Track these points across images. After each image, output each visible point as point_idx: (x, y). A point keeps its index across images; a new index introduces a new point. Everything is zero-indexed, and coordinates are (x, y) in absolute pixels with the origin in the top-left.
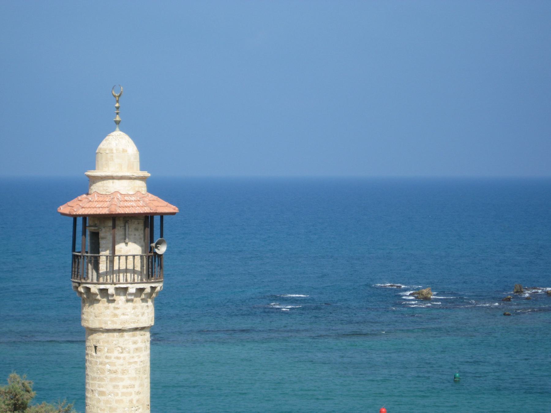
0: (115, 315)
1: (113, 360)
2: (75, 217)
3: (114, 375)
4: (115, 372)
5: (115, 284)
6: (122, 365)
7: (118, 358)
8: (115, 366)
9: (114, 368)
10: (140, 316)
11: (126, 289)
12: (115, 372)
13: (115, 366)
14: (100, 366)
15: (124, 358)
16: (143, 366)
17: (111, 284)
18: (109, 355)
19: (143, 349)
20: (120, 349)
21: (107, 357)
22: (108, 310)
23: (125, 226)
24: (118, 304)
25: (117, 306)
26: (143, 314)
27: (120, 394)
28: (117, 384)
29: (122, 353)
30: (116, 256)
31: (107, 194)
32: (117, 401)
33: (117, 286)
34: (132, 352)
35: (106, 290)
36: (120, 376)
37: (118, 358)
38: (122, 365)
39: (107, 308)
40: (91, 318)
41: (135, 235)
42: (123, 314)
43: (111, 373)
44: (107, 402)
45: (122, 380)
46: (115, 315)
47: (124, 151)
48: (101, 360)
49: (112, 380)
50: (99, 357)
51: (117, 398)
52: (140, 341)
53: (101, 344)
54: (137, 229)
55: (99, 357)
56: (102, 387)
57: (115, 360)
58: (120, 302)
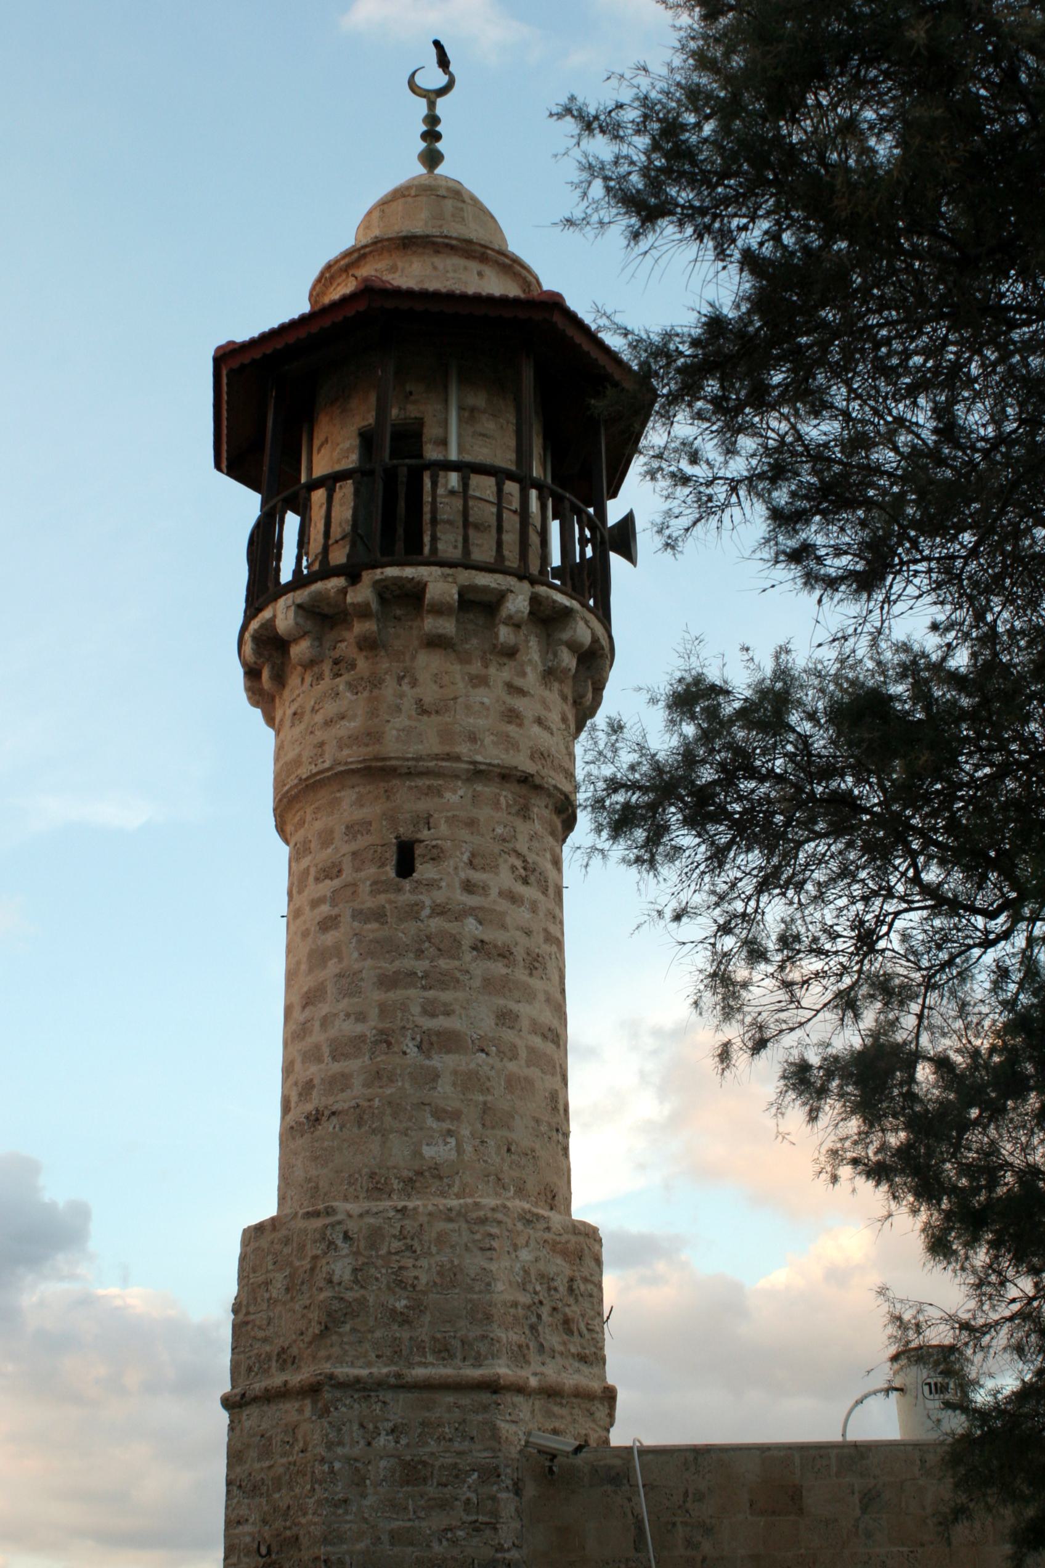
1: (492, 900)
3: (498, 968)
7: (513, 898)
8: (504, 927)
13: (504, 927)
18: (477, 876)
21: (469, 887)
22: (481, 691)
24: (524, 674)
25: (518, 682)
32: (512, 1083)
35: (501, 596)
36: (520, 974)
39: (480, 681)
40: (401, 721)
43: (489, 956)
44: (470, 1081)
46: (513, 716)
48: (439, 896)
49: (491, 985)
50: (431, 885)
51: (512, 1067)
53: (443, 828)
55: (431, 885)
56: (447, 1014)
57: (504, 905)
58: (528, 669)
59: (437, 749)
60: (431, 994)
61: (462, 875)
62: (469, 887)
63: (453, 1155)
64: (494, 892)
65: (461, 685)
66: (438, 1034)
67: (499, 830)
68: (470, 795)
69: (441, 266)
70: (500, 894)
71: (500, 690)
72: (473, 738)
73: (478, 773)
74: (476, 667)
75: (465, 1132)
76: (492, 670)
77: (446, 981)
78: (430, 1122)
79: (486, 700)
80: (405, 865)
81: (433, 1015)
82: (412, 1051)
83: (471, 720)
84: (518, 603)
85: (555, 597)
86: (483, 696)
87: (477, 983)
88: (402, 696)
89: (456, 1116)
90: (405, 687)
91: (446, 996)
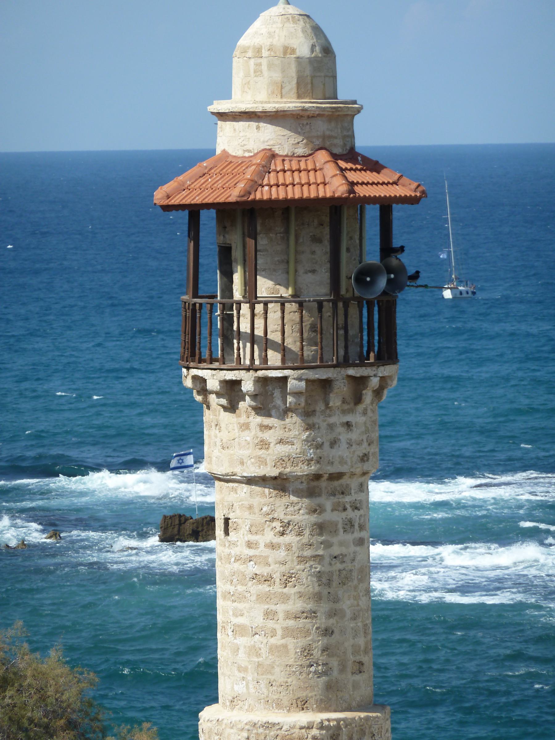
0: (264, 445)
1: (262, 550)
2: (194, 212)
3: (265, 588)
4: (268, 579)
5: (256, 370)
6: (284, 563)
7: (273, 546)
9: (264, 571)
10: (327, 445)
11: (285, 379)
12: (268, 579)
14: (237, 566)
15: (289, 548)
16: (339, 566)
17: (248, 370)
19: (340, 526)
20: (277, 524)
21: (249, 545)
22: (247, 432)
23: (287, 232)
26: (333, 443)
27: (279, 632)
28: (273, 607)
29: (282, 534)
30: (259, 303)
31: (247, 155)
33: (261, 373)
34: (307, 532)
35: (238, 383)
37: (273, 546)
38: (284, 563)
39: (245, 427)
41: (313, 253)
42: (281, 441)
43: (259, 582)
45: (285, 598)
46: (264, 445)
47: (287, 50)
50: (235, 544)
52: (328, 505)
53: (238, 511)
54: (317, 240)
55: (235, 544)
59: (229, 470)
60: (235, 604)
61: (246, 539)
62: (249, 545)
63: (245, 690)
64: (262, 545)
65: (236, 431)
66: (239, 626)
67: (265, 509)
68: (249, 491)
69: (237, 128)
70: (266, 546)
71: (254, 431)
72: (242, 463)
73: (250, 481)
74: (243, 419)
75: (250, 678)
76: (251, 418)
77: (241, 598)
78: (236, 672)
79: (248, 439)
80: (227, 533)
81: (237, 616)
82: (230, 633)
83: (241, 452)
84: (248, 386)
85: (270, 375)
86: (248, 436)
87: (254, 598)
88: (216, 437)
89: (245, 670)
90: (217, 431)
91: (240, 606)
